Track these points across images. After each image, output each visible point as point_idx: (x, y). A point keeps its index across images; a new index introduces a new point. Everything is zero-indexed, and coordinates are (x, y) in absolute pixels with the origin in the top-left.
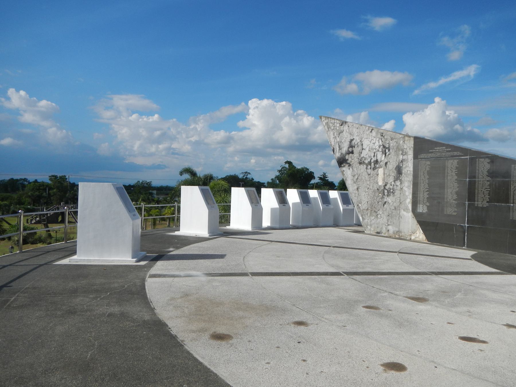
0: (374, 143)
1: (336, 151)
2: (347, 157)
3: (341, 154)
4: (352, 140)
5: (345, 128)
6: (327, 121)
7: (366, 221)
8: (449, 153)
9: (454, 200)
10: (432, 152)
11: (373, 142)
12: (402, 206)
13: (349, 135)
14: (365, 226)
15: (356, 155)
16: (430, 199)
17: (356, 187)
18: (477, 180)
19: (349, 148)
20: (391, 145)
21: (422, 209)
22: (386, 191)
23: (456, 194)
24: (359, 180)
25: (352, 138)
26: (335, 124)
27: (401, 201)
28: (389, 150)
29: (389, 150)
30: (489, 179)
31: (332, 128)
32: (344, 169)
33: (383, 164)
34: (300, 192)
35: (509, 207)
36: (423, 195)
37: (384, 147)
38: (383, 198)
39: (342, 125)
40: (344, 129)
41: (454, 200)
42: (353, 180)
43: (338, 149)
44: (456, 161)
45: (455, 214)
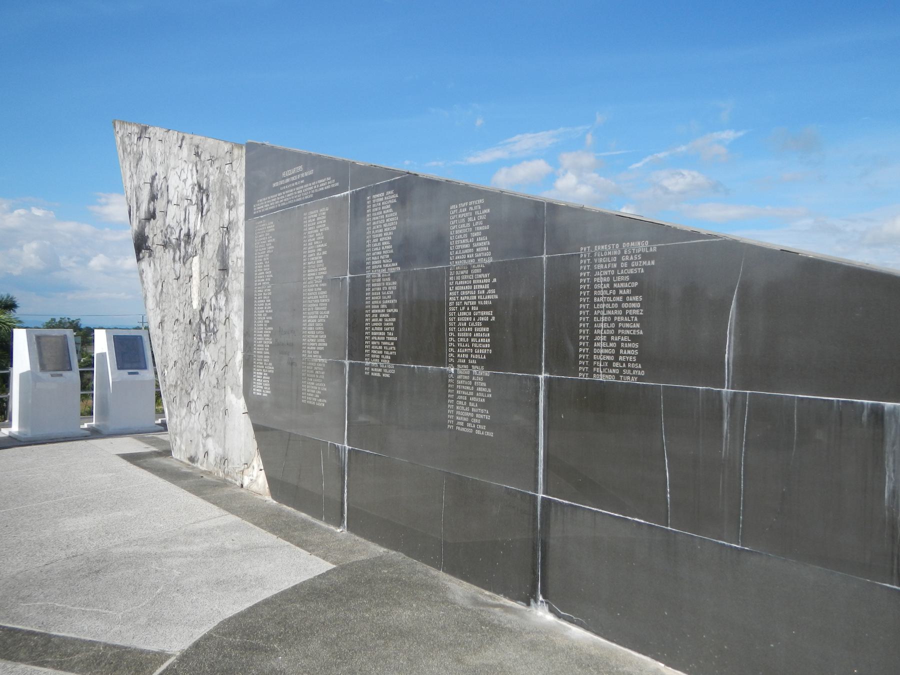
0: (185, 181)
7: (174, 420)
8: (310, 187)
9: (321, 352)
10: (277, 190)
11: (183, 177)
12: (229, 375)
14: (173, 437)
15: (158, 222)
16: (277, 348)
17: (159, 319)
18: (368, 275)
19: (149, 203)
21: (262, 387)
22: (203, 328)
23: (326, 331)
24: (164, 295)
27: (227, 361)
30: (395, 268)
32: (144, 265)
33: (197, 240)
34: (38, 338)
35: (445, 375)
36: (264, 339)
37: (200, 188)
38: (198, 349)
41: (321, 352)
42: (154, 296)
44: (324, 211)
45: (322, 403)
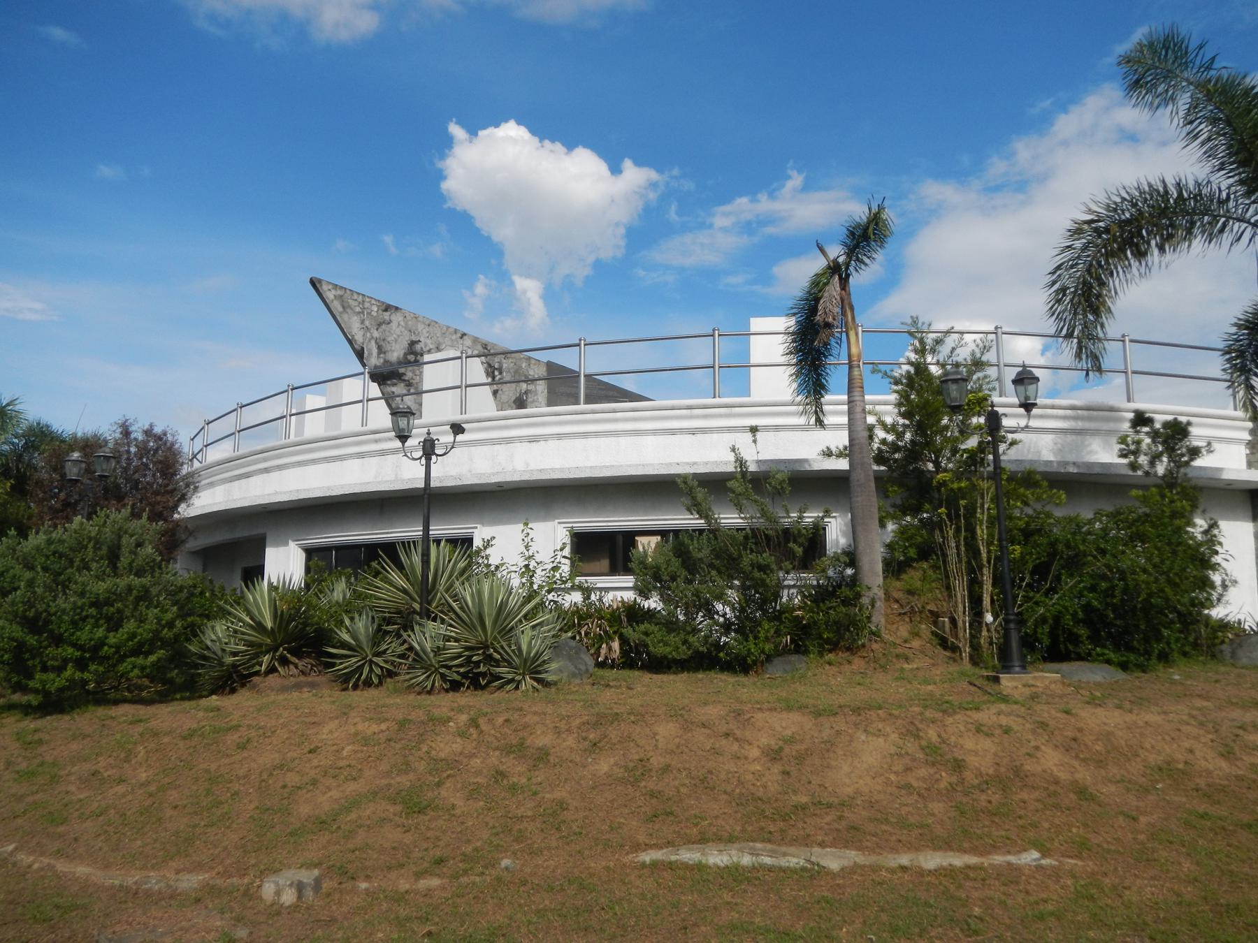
1: (370, 354)
2: (402, 370)
3: (386, 361)
4: (412, 343)
5: (397, 318)
6: (339, 292)
13: (406, 333)
19: (405, 354)
20: (505, 366)
25: (414, 338)
26: (367, 305)
28: (501, 373)
29: (501, 373)
31: (358, 309)
39: (386, 310)
40: (393, 318)
43: (375, 351)
